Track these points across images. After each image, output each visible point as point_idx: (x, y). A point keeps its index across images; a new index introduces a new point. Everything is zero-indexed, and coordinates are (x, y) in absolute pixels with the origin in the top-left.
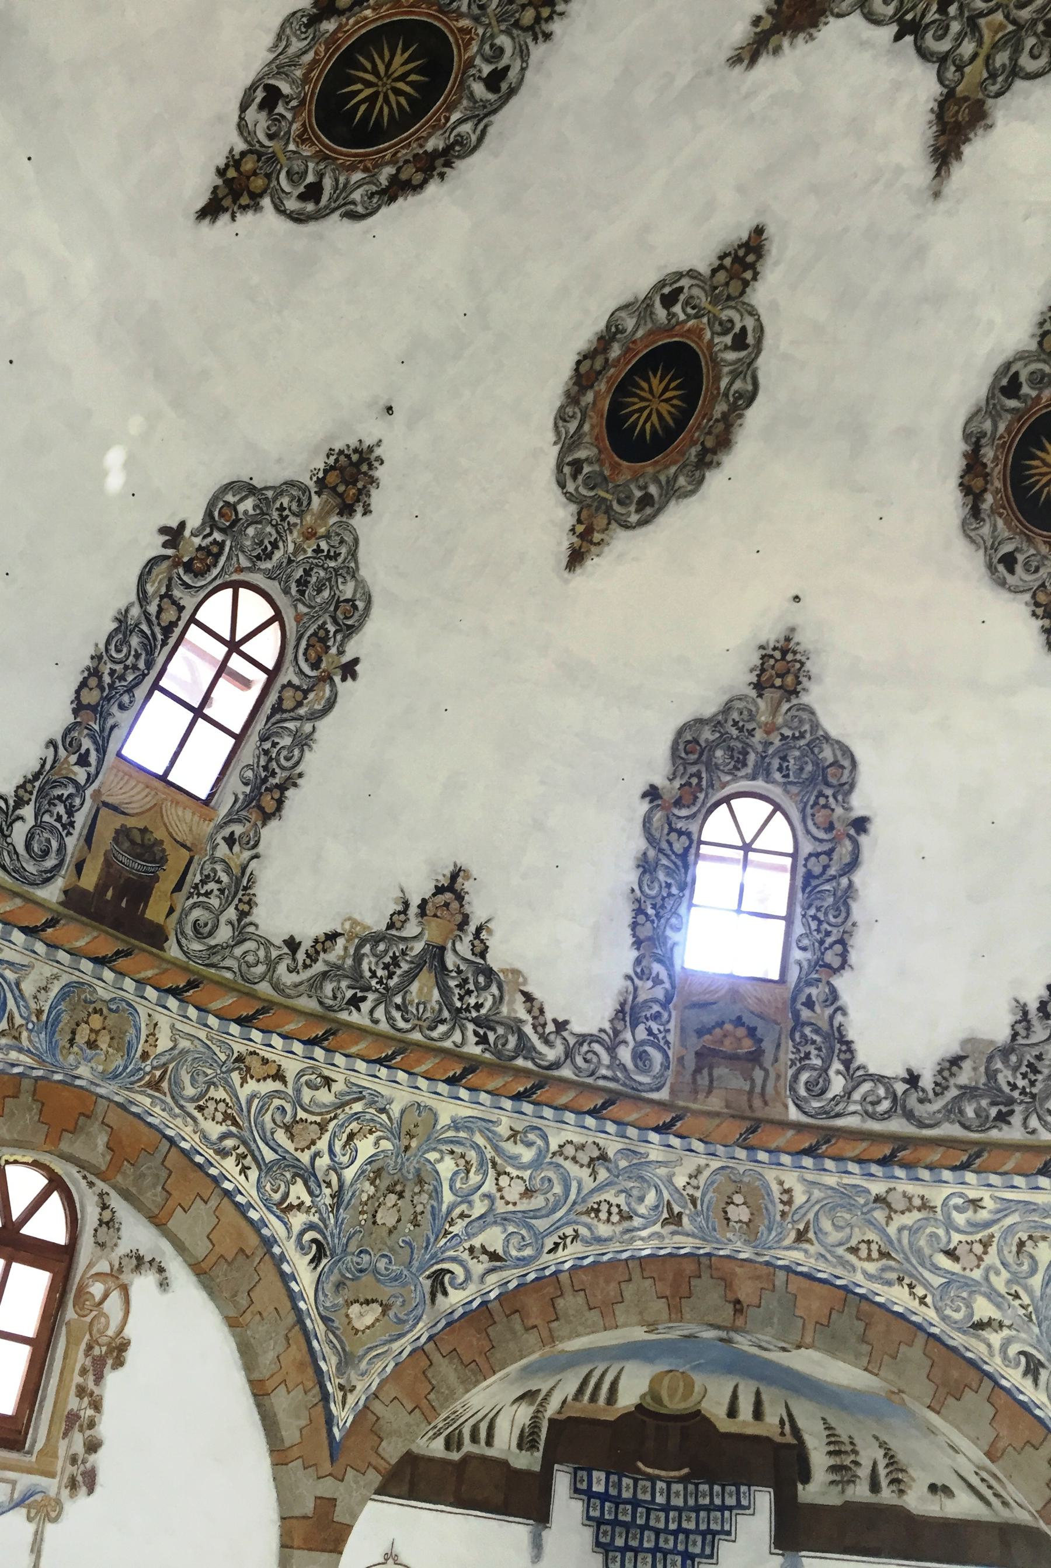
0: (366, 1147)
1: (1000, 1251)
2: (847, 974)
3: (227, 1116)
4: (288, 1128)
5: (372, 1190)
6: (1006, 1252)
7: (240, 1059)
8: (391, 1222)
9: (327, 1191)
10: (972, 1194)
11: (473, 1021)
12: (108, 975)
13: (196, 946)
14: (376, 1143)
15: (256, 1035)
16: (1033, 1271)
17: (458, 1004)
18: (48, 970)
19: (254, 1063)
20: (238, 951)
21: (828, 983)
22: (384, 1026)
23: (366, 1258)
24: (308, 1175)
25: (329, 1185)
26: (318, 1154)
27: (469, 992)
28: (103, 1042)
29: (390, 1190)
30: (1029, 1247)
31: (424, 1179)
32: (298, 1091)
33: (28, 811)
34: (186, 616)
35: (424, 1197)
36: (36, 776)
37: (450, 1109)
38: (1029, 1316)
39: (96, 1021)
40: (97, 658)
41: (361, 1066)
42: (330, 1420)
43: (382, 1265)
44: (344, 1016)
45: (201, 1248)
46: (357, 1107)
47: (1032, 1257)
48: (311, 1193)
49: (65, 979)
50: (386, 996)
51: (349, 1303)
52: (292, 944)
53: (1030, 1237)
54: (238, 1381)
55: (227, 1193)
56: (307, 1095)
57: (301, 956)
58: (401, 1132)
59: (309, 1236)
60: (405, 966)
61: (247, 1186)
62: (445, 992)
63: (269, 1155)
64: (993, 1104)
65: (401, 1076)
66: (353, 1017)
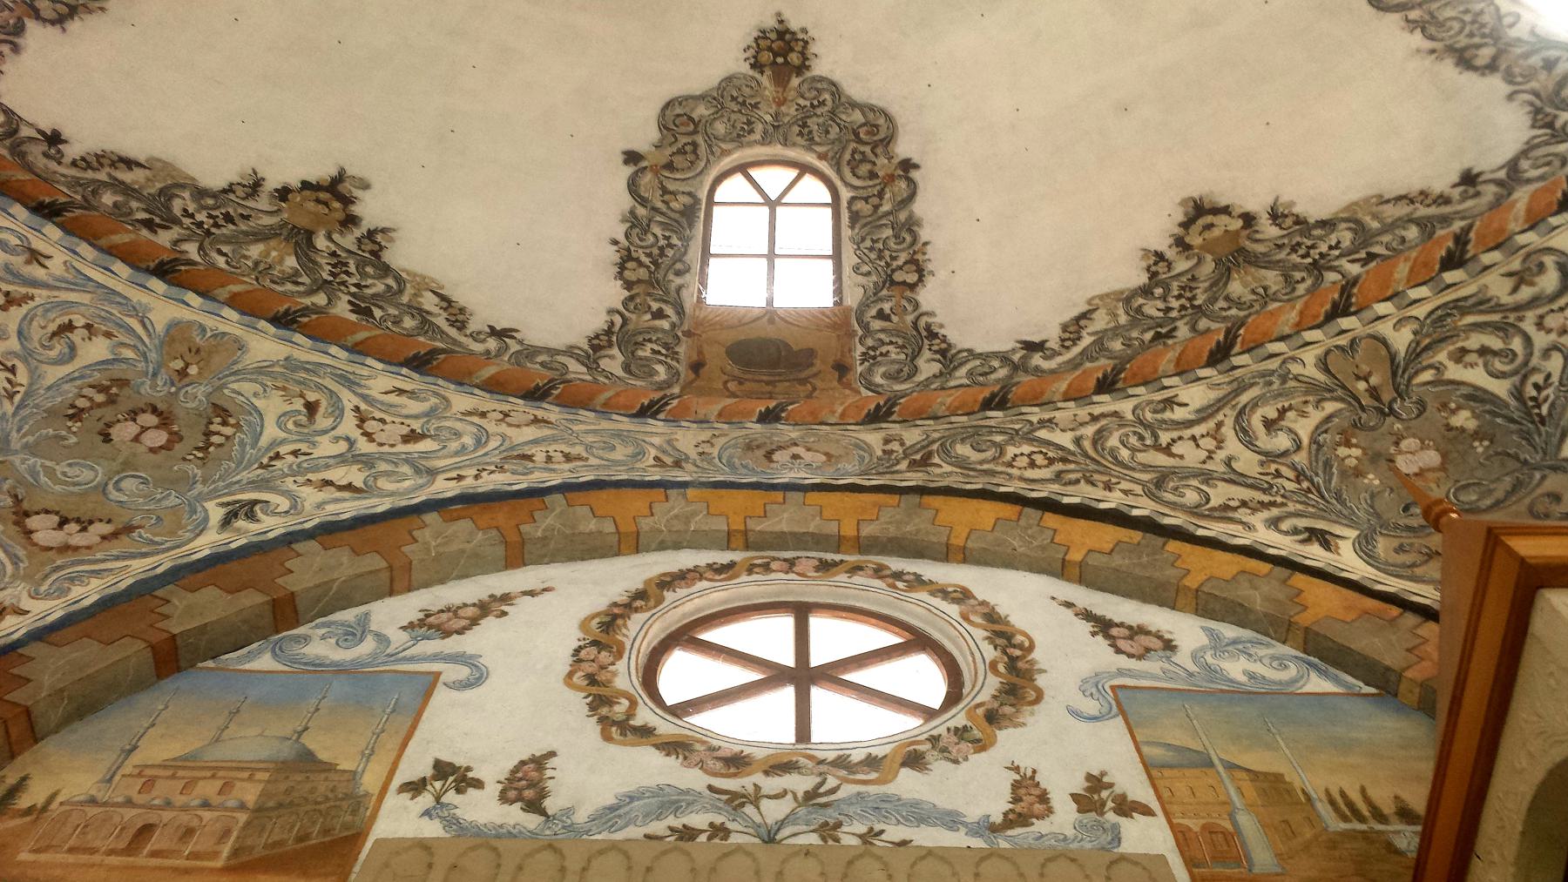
1: (28, 319)
2: (52, 32)
6: (35, 323)
10: (38, 244)
16: (60, 361)
21: (20, 19)
30: (77, 336)
38: (11, 396)
47: (73, 348)
53: (88, 327)
64: (146, 210)
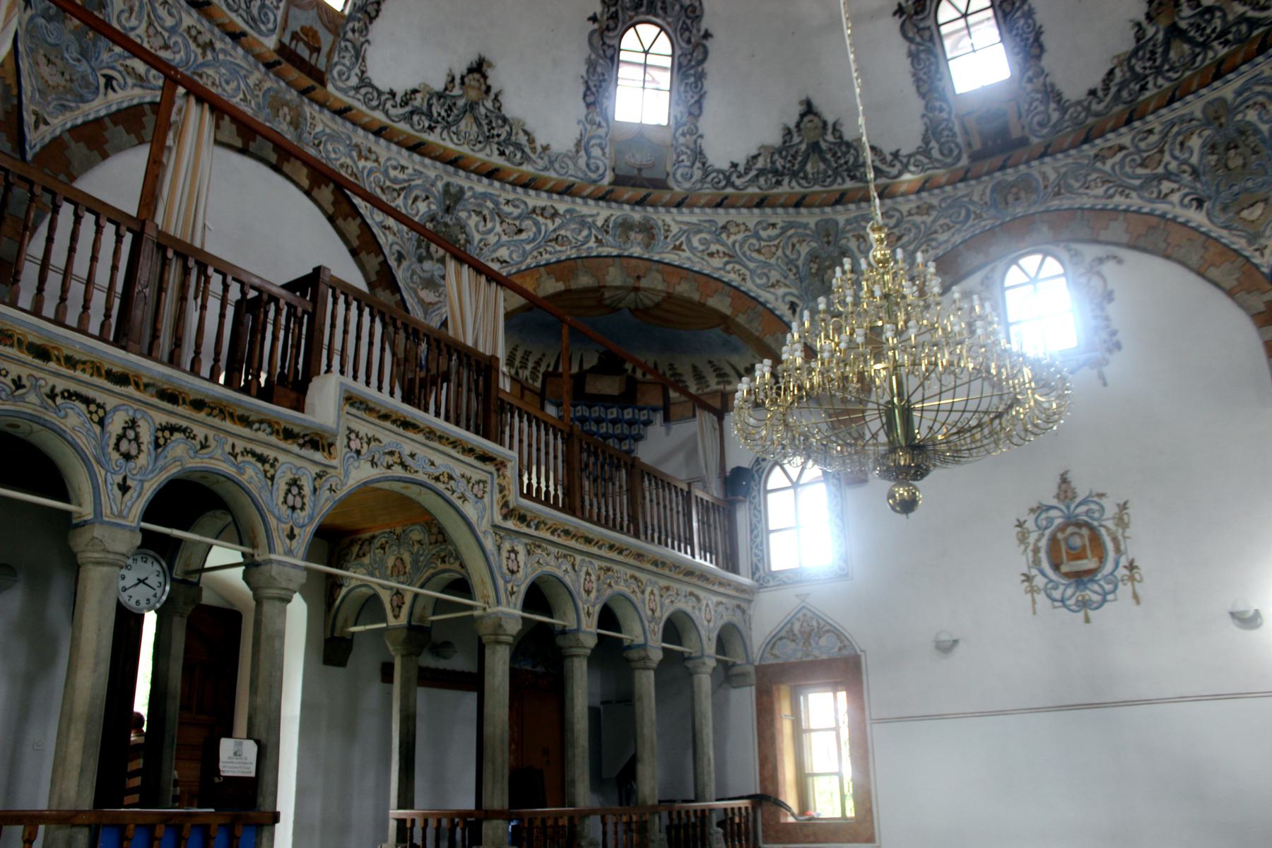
0: (1195, 142)
3: (1104, 182)
4: (1142, 165)
5: (1215, 157)
7: (1096, 156)
8: (1240, 161)
9: (1186, 175)
11: (1216, 39)
12: (1010, 171)
13: (1045, 131)
14: (1200, 135)
15: (1098, 141)
17: (1202, 39)
18: (981, 187)
19: (1106, 153)
20: (1067, 117)
22: (1167, 85)
23: (1236, 189)
24: (1168, 176)
25: (1184, 172)
26: (1167, 164)
27: (1204, 29)
28: (1022, 195)
29: (1228, 149)
31: (1244, 131)
32: (1137, 146)
33: (933, 144)
34: (933, 27)
35: (1252, 138)
36: (927, 131)
37: (1227, 90)
39: (1014, 190)
40: (914, 75)
41: (1163, 111)
42: (1257, 267)
43: (1250, 184)
44: (1141, 98)
45: (1125, 239)
46: (1175, 129)
48: (1175, 182)
49: (990, 185)
50: (1158, 71)
51: (1239, 212)
52: (1093, 93)
54: (1192, 278)
55: (1126, 211)
56: (1143, 145)
57: (1100, 93)
58: (1207, 123)
59: (1187, 200)
60: (1160, 50)
61: (1135, 201)
62: (1191, 41)
63: (1137, 182)
65: (1189, 98)
66: (1147, 94)
